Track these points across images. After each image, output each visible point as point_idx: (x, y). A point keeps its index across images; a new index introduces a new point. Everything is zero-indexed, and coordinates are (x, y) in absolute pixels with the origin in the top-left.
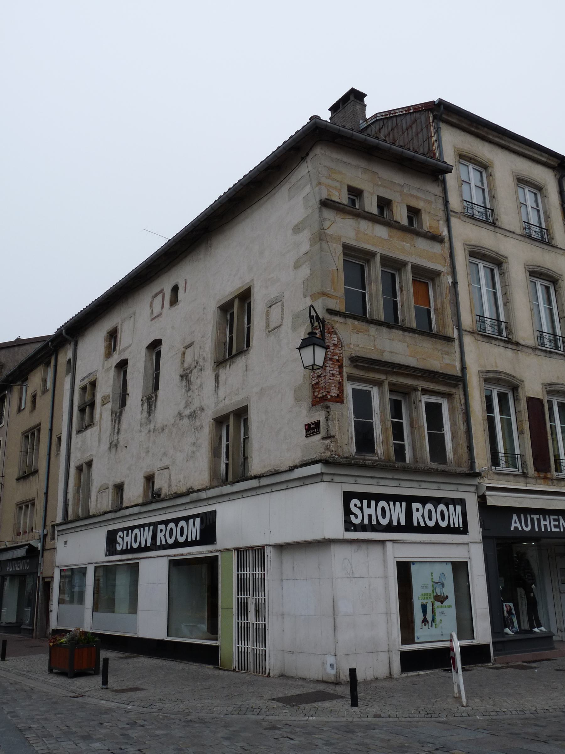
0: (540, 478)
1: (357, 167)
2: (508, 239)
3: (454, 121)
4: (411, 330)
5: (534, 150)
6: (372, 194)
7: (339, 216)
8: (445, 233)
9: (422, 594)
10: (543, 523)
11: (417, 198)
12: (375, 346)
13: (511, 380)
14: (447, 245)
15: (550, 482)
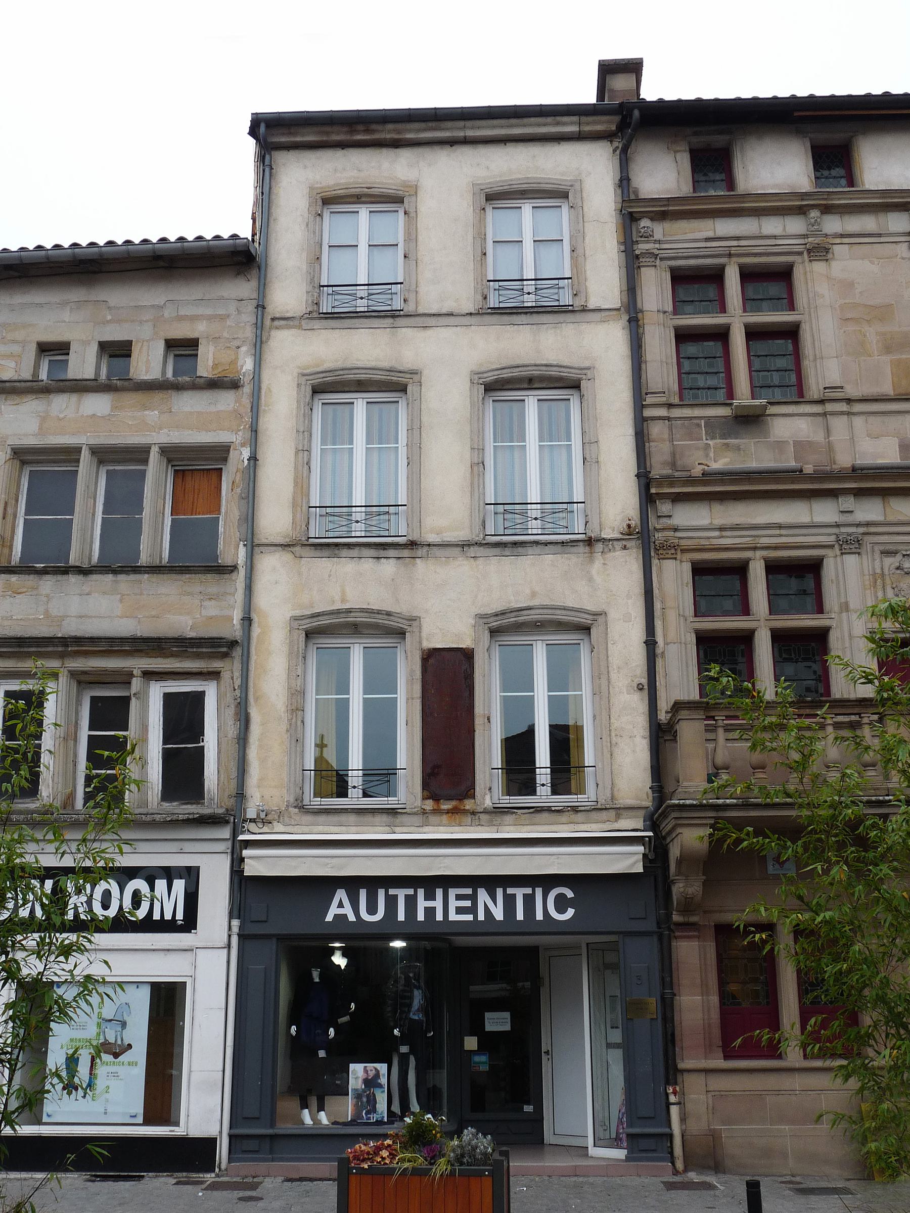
0: (437, 811)
1: (63, 304)
2: (429, 332)
3: (311, 138)
4: (129, 569)
5: (533, 120)
6: (85, 343)
7: (9, 402)
8: (247, 365)
9: (72, 1040)
10: (422, 904)
11: (193, 319)
12: (47, 611)
13: (380, 621)
14: (247, 389)
15: (468, 819)
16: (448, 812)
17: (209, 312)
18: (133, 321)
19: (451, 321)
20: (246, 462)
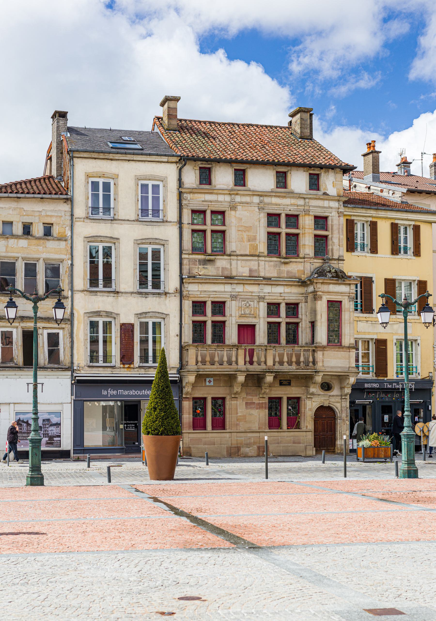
0: (124, 368)
8: (69, 234)
16: (127, 368)
17: (56, 214)
18: (32, 216)
19: (128, 222)
20: (70, 265)
